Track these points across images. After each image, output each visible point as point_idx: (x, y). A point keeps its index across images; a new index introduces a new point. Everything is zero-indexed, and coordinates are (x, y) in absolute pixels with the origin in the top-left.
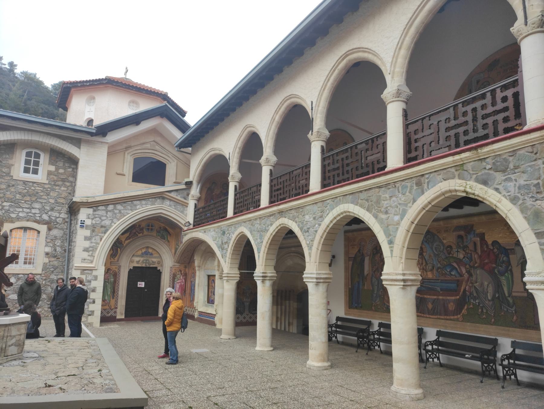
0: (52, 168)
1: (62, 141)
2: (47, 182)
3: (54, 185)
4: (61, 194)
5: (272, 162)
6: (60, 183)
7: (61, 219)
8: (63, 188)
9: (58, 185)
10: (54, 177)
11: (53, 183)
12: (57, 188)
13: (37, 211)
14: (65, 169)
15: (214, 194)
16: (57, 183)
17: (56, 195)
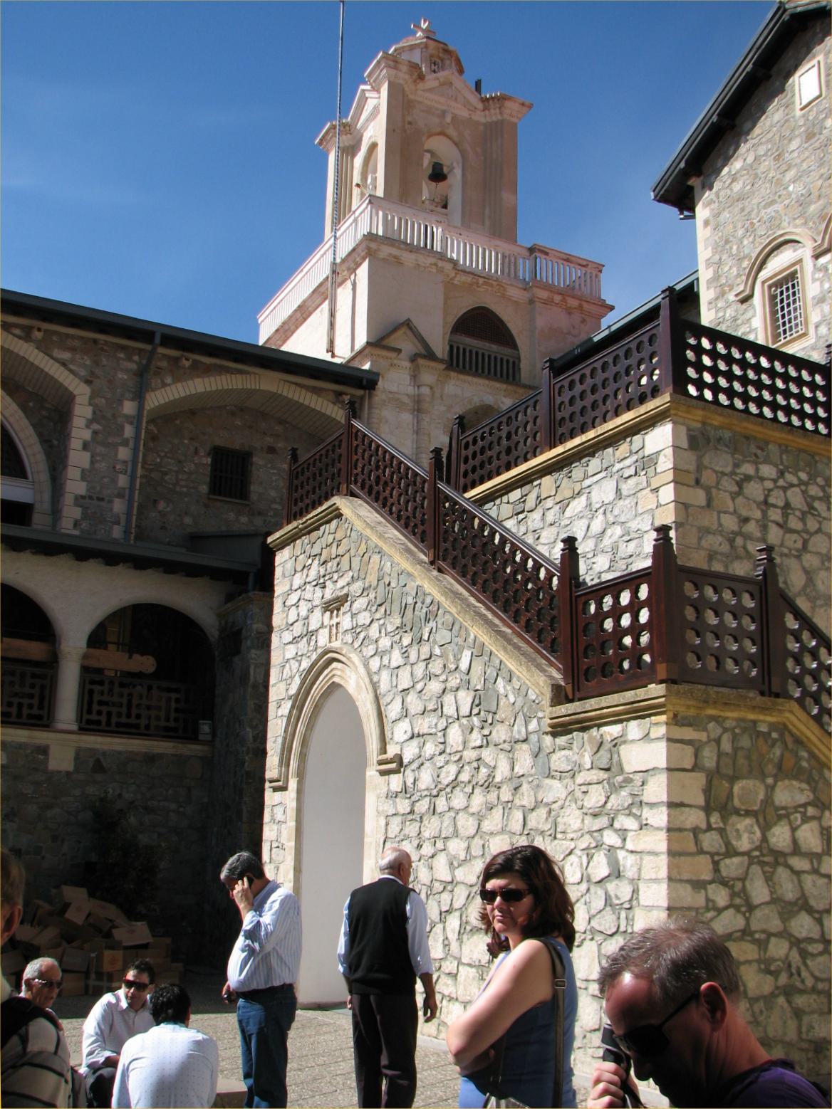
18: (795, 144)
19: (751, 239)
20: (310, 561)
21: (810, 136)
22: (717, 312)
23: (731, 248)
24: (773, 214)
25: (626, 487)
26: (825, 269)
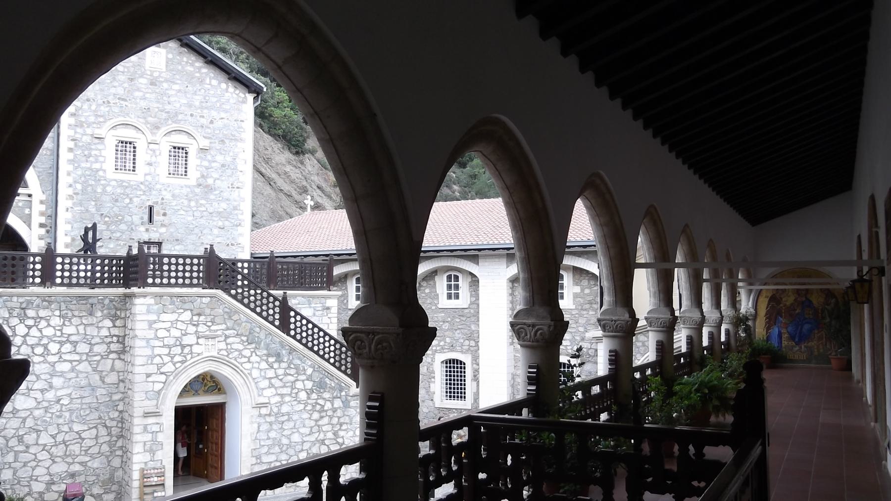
0: (577, 289)
1: (577, 258)
2: (573, 307)
3: (582, 309)
4: (590, 320)
5: (711, 321)
6: (587, 306)
7: (593, 351)
8: (591, 313)
9: (586, 310)
10: (580, 299)
11: (580, 308)
12: (585, 312)
13: (569, 344)
14: (590, 288)
15: (781, 305)
16: (584, 308)
17: (584, 322)
18: (142, 80)
19: (107, 109)
20: (182, 311)
21: (152, 83)
22: (76, 132)
23: (91, 105)
24: (124, 105)
25: (317, 313)
26: (154, 151)
